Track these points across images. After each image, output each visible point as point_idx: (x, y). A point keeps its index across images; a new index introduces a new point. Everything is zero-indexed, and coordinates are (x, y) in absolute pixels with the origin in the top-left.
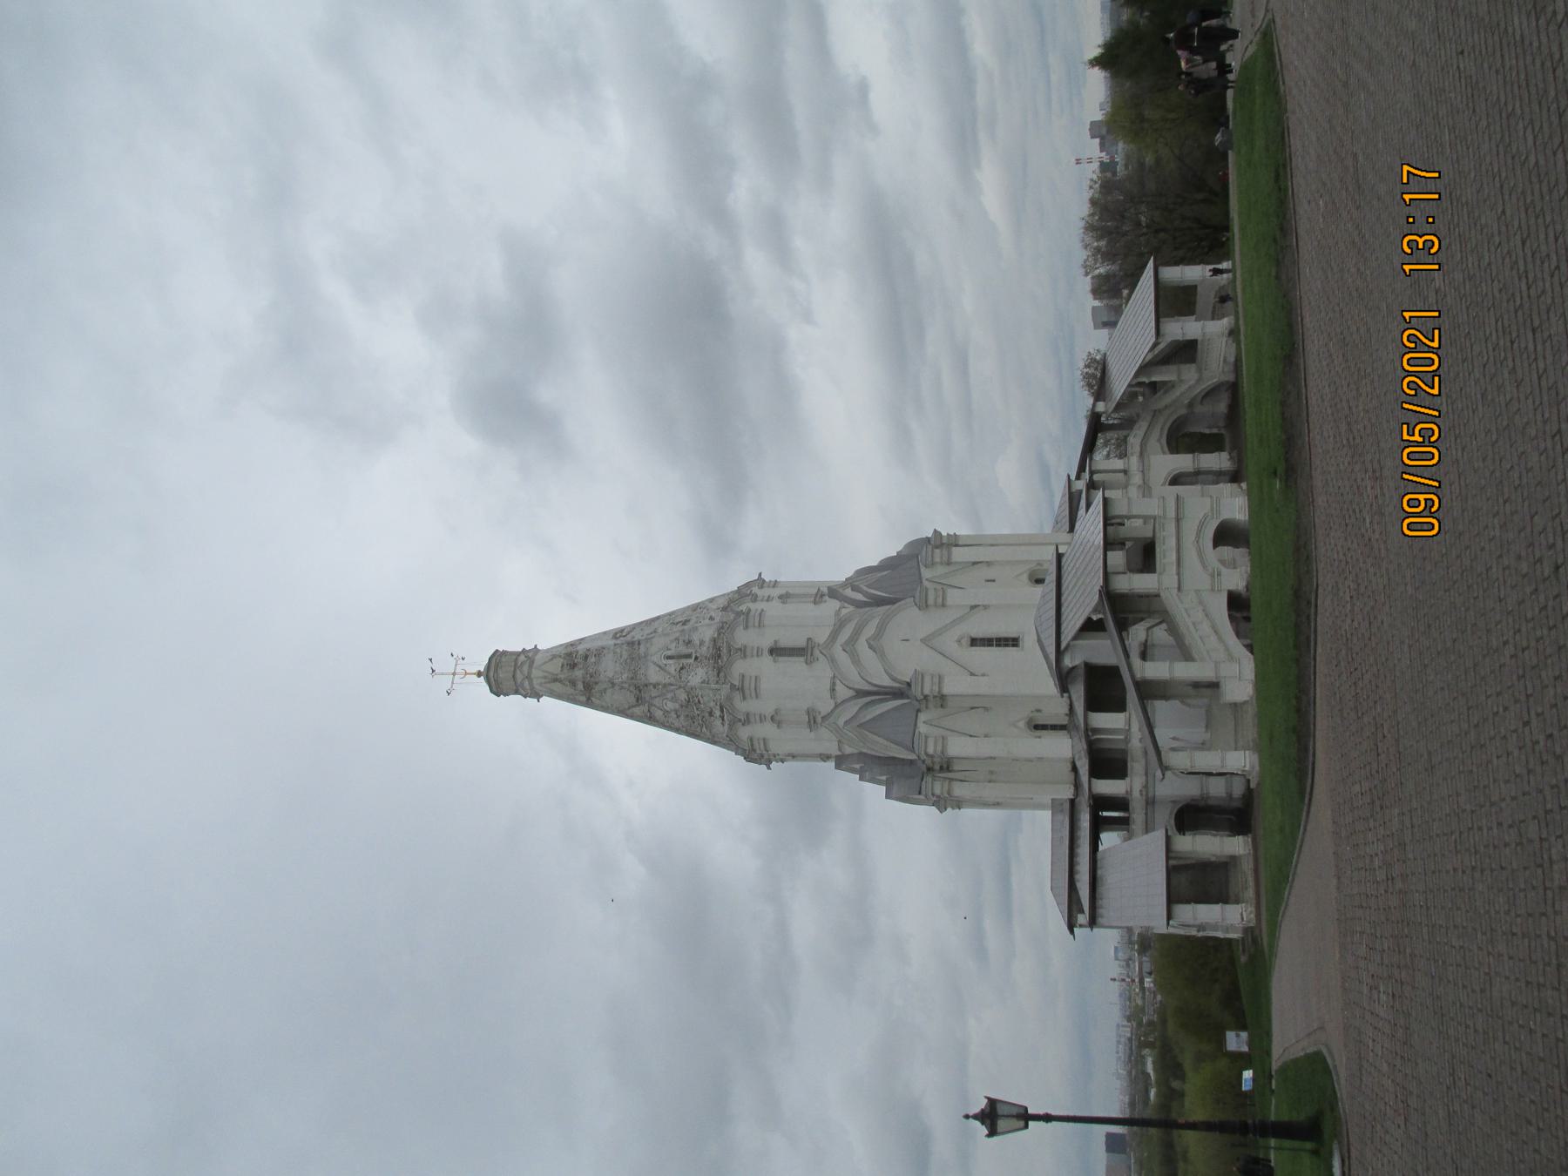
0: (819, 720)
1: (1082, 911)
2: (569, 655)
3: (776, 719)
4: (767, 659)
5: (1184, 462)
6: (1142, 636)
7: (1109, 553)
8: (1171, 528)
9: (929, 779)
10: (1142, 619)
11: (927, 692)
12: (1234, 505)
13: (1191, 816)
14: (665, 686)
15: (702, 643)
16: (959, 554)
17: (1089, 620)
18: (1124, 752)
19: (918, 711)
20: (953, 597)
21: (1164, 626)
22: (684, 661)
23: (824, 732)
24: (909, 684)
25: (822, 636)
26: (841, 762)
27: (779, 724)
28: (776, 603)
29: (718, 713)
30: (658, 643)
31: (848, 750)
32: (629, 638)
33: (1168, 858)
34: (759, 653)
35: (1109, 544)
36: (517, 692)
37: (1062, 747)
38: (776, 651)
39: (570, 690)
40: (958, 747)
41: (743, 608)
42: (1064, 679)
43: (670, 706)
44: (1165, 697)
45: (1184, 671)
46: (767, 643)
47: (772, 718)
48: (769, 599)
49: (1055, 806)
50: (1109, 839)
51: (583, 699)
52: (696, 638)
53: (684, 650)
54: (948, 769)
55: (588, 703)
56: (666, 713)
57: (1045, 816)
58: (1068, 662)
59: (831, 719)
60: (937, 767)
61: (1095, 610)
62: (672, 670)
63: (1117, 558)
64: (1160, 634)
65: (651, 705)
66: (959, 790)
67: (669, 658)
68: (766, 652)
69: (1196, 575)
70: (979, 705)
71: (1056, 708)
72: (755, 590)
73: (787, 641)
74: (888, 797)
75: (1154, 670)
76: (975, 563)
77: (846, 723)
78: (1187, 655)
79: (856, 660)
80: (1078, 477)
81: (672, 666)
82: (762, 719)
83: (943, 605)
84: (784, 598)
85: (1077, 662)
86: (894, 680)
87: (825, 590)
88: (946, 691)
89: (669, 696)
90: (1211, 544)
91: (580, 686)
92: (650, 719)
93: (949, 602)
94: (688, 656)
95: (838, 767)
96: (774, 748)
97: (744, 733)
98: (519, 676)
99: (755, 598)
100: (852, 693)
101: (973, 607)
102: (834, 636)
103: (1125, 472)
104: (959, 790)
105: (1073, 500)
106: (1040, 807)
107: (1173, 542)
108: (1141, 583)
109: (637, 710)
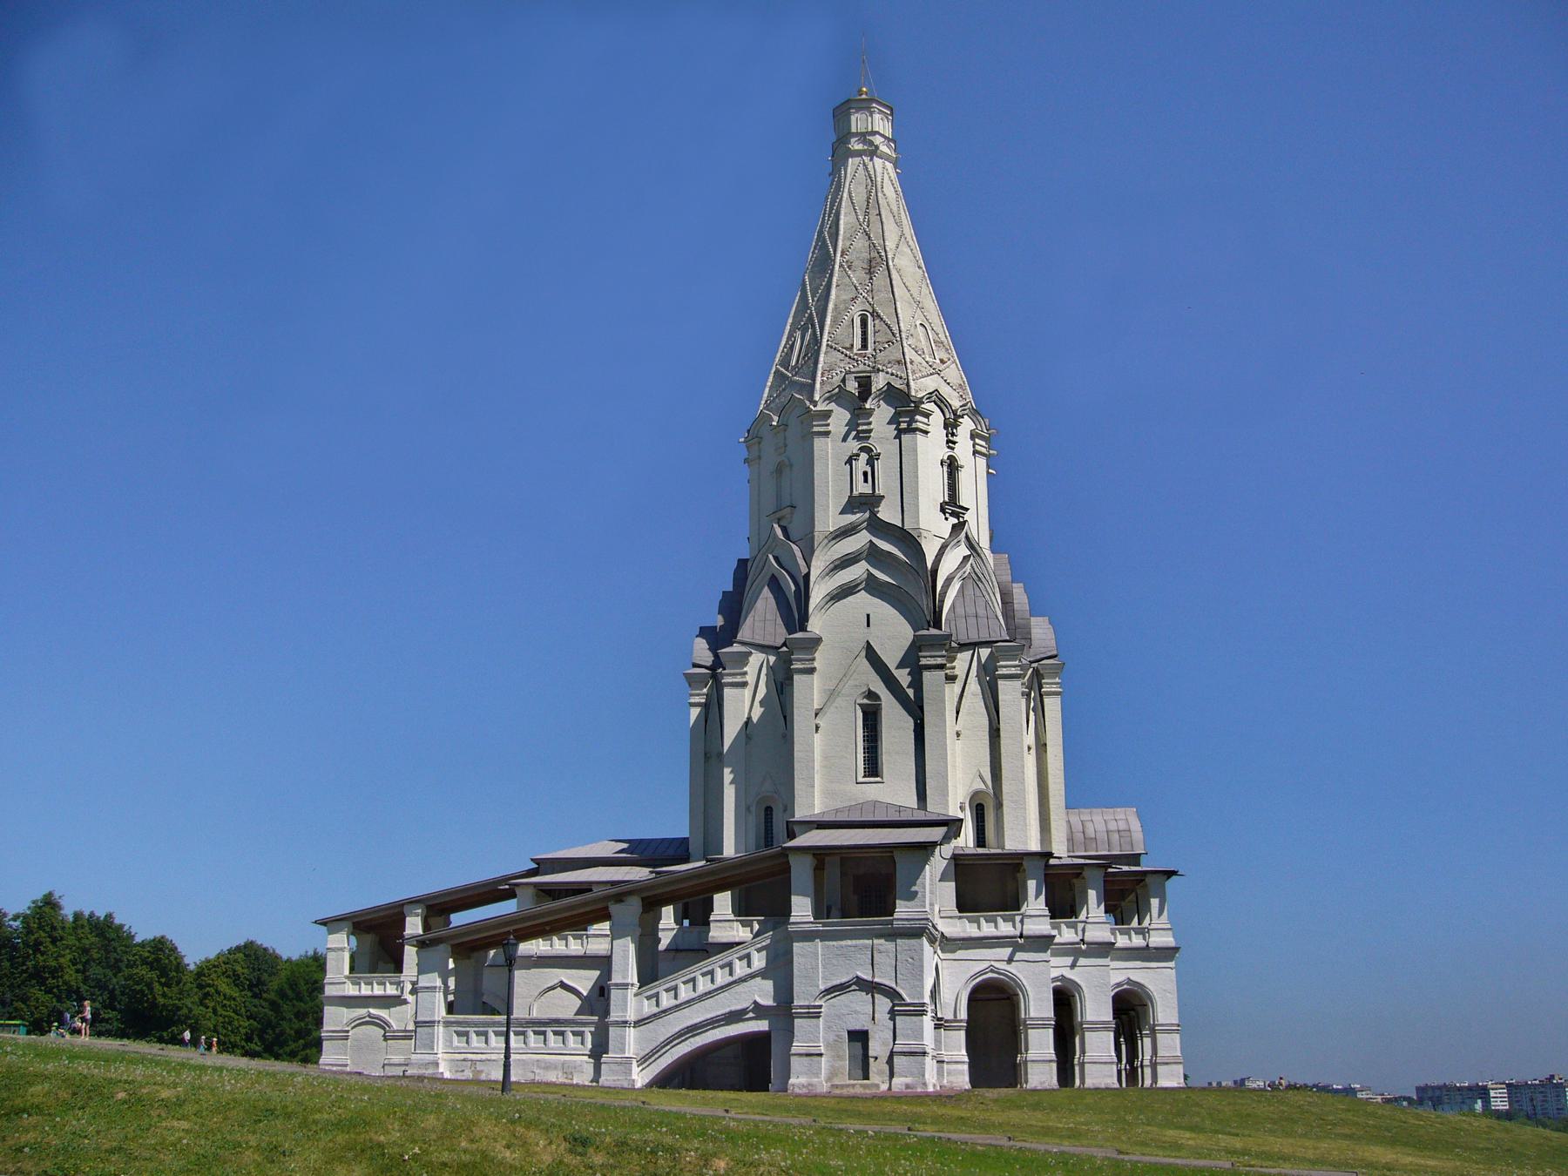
16: (1011, 694)
25: (888, 513)
48: (950, 443)
72: (967, 425)
84: (952, 466)
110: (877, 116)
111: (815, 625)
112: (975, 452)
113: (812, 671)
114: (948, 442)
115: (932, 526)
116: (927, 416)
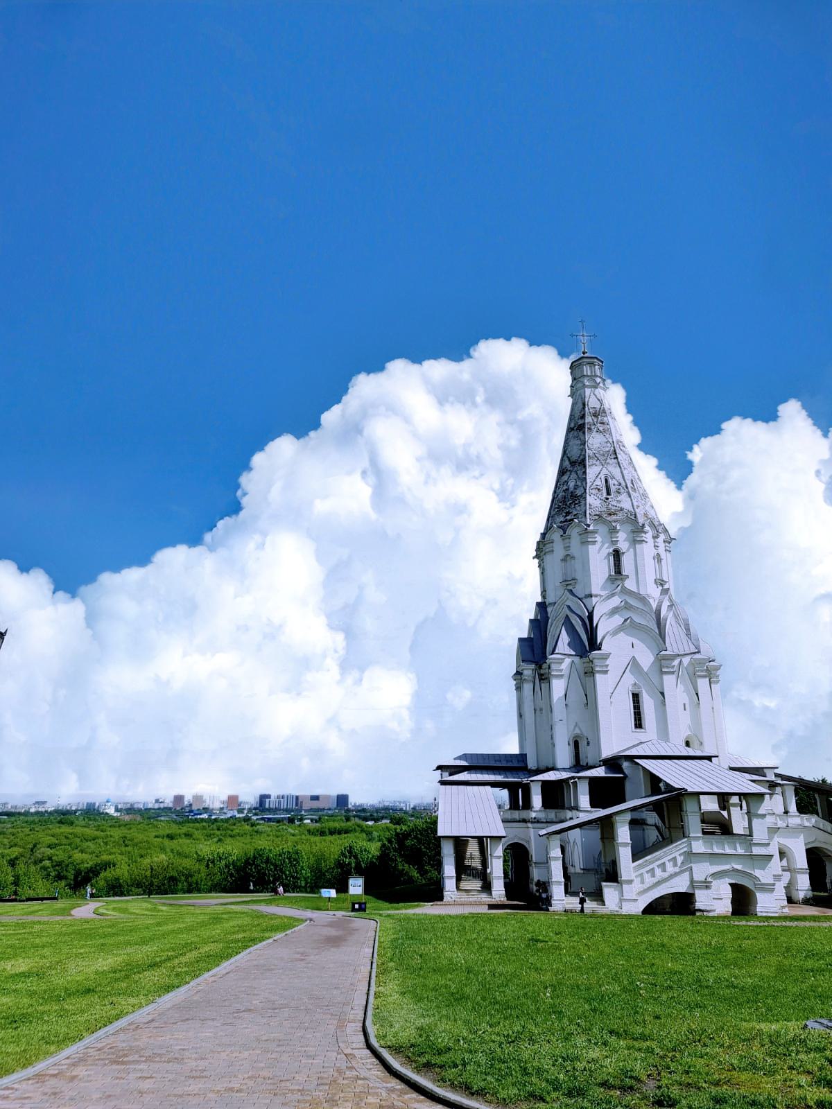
1: (450, 775)
2: (604, 412)
3: (567, 558)
5: (801, 861)
6: (650, 821)
7: (716, 797)
8: (740, 851)
9: (533, 666)
10: (664, 823)
11: (595, 661)
12: (769, 903)
13: (518, 856)
14: (585, 479)
15: (619, 501)
16: (703, 684)
17: (660, 780)
18: (562, 807)
19: (581, 657)
20: (669, 680)
21: (661, 840)
22: (604, 491)
24: (600, 649)
25: (630, 584)
26: (542, 606)
27: (564, 560)
28: (654, 552)
29: (568, 518)
30: (616, 472)
31: (549, 610)
32: (617, 451)
33: (487, 837)
35: (723, 798)
36: (574, 379)
38: (617, 554)
39: (577, 415)
40: (558, 687)
41: (647, 528)
42: (613, 763)
43: (572, 484)
44: (602, 838)
45: (624, 854)
46: (623, 545)
49: (522, 757)
50: (505, 794)
51: (572, 425)
52: (623, 497)
53: (613, 489)
54: (540, 680)
55: (570, 430)
56: (567, 482)
57: (514, 750)
58: (625, 765)
59: (571, 597)
60: (542, 672)
61: (667, 785)
62: (598, 482)
63: (710, 805)
64: (652, 835)
65: (571, 471)
66: (528, 687)
67: (606, 481)
68: (615, 547)
69: (702, 871)
70: (589, 701)
71: (588, 755)
72: (662, 536)
73: (627, 561)
74: (521, 640)
75: (623, 833)
76: (697, 694)
77: (569, 607)
78: (636, 856)
79: (614, 611)
80: (777, 775)
81: (600, 483)
82: (567, 548)
83: (662, 673)
84: (658, 558)
85: (626, 771)
86: (603, 638)
87: (666, 587)
88: (598, 676)
89: (579, 483)
90: (733, 882)
91: (580, 422)
92: (562, 472)
93: (665, 677)
94: (608, 493)
95: (538, 604)
96: (548, 558)
97: (556, 536)
99: (655, 537)
100: (590, 610)
101: (662, 694)
102: (630, 593)
103: (786, 812)
104: (528, 687)
105: (758, 771)
106: (521, 746)
107: (729, 850)
108: (693, 824)
109: (567, 463)
110: (597, 367)
111: (605, 648)
112: (666, 550)
113: (606, 672)
114: (655, 546)
115: (653, 592)
116: (645, 533)
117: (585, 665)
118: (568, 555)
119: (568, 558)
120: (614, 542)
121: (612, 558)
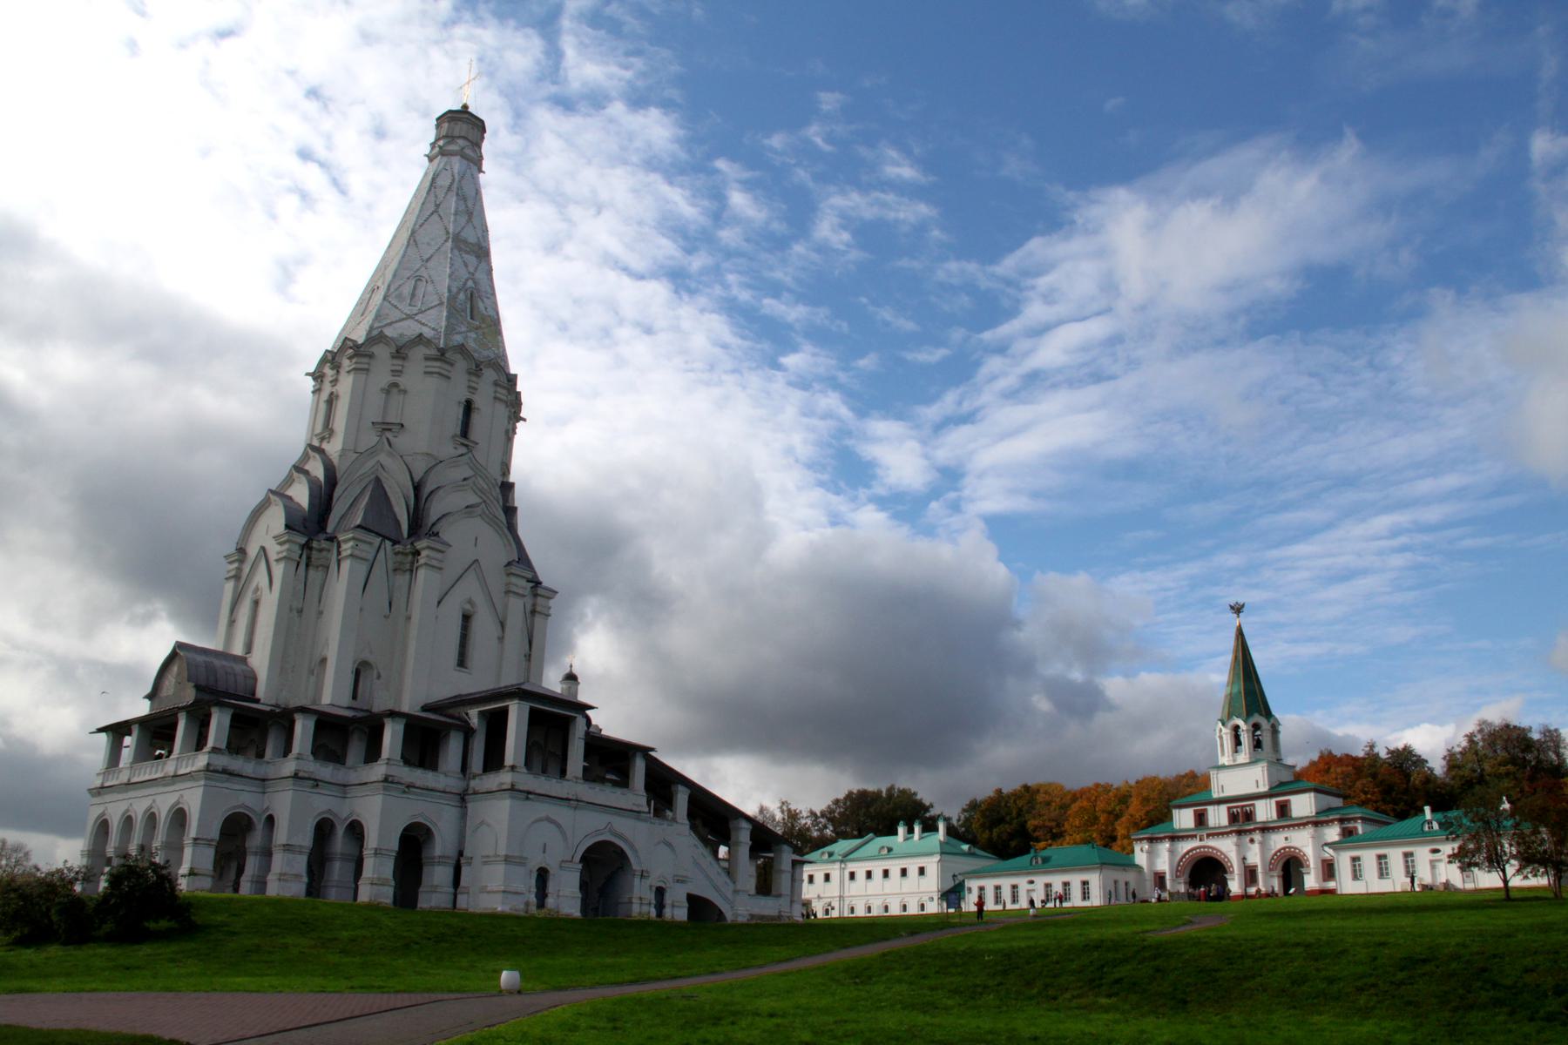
0: (389, 435)
4: (464, 395)
23: (370, 438)
34: (472, 389)
37: (332, 694)
38: (468, 407)
47: (395, 385)
68: (469, 396)
93: (513, 600)
98: (461, 142)
101: (502, 625)
117: (400, 558)
118: (395, 385)
119: (395, 390)
120: (472, 389)
121: (461, 411)
